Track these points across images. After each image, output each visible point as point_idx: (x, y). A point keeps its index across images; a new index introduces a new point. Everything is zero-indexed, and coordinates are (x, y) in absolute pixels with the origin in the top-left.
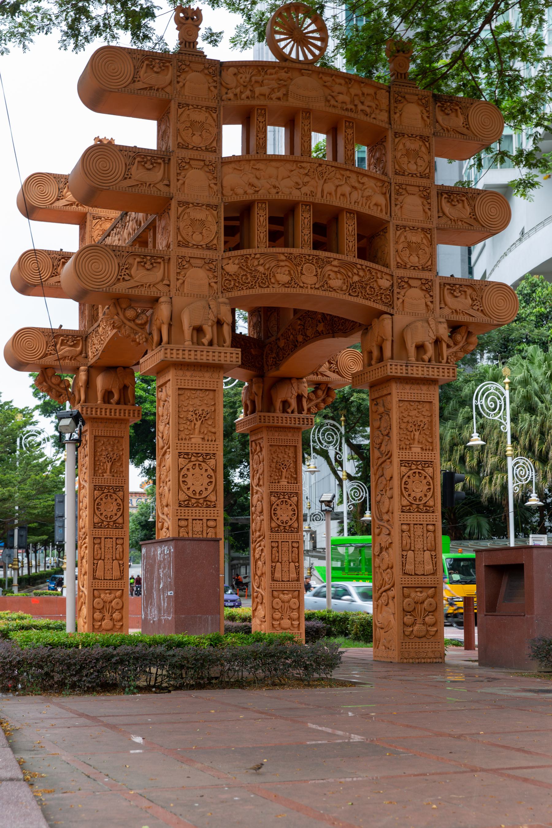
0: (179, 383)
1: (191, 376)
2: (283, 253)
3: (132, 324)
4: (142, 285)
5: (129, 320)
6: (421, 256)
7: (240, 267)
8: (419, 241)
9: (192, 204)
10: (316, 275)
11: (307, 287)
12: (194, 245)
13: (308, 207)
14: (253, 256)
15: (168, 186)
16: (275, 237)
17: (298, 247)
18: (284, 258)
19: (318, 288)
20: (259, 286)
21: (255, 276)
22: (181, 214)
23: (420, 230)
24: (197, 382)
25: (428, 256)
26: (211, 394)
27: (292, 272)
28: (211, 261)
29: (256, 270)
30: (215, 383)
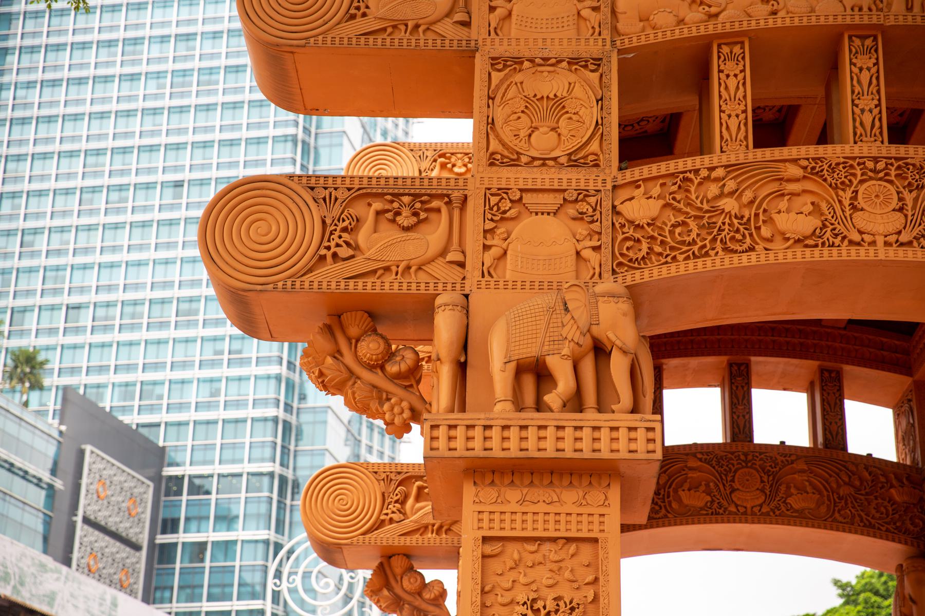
0: (485, 524)
1: (522, 502)
2: (795, 161)
3: (376, 378)
4: (387, 269)
5: (371, 368)
7: (666, 205)
9: (531, 61)
10: (901, 210)
11: (873, 243)
12: (534, 159)
13: (869, 42)
14: (704, 173)
15: (466, 24)
16: (772, 128)
17: (843, 141)
18: (799, 172)
19: (910, 243)
20: (726, 250)
21: (711, 225)
22: (498, 87)
24: (540, 518)
26: (586, 549)
27: (824, 206)
28: (583, 195)
29: (714, 209)
30: (596, 519)
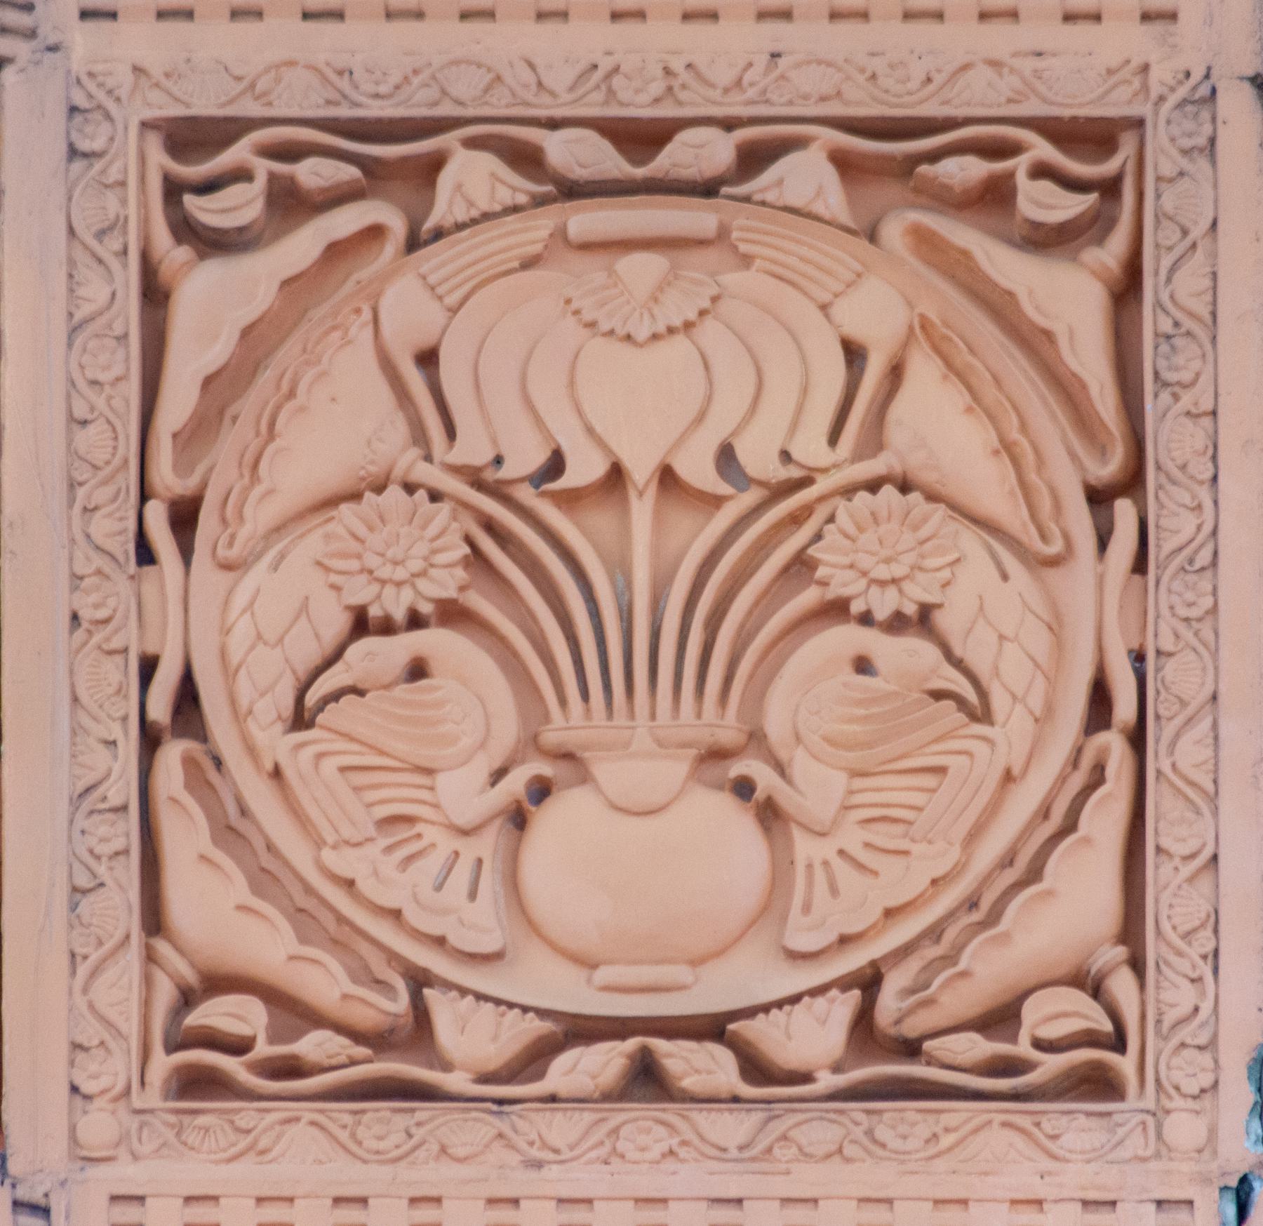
6: (814, 787)
8: (787, 422)
23: (805, 176)
25: (1033, 736)
